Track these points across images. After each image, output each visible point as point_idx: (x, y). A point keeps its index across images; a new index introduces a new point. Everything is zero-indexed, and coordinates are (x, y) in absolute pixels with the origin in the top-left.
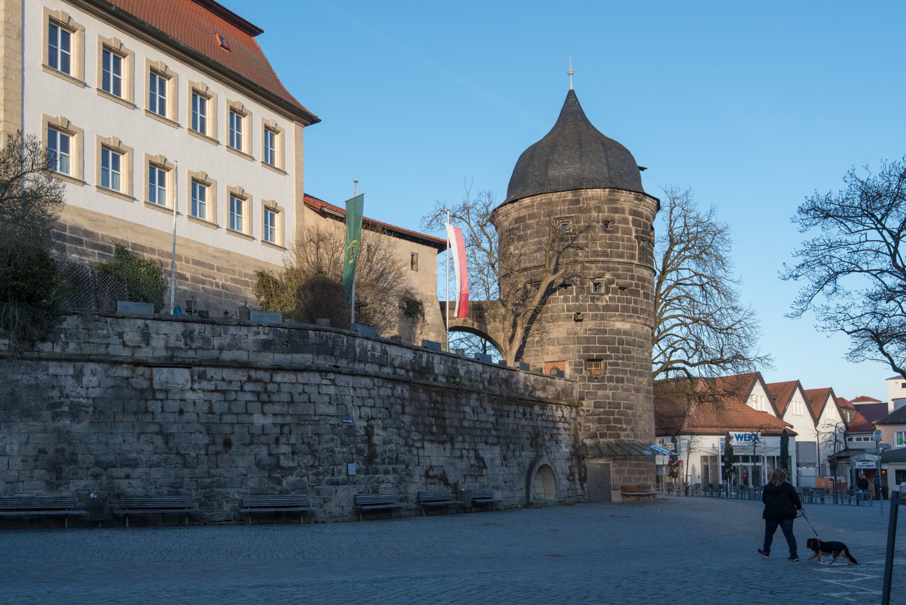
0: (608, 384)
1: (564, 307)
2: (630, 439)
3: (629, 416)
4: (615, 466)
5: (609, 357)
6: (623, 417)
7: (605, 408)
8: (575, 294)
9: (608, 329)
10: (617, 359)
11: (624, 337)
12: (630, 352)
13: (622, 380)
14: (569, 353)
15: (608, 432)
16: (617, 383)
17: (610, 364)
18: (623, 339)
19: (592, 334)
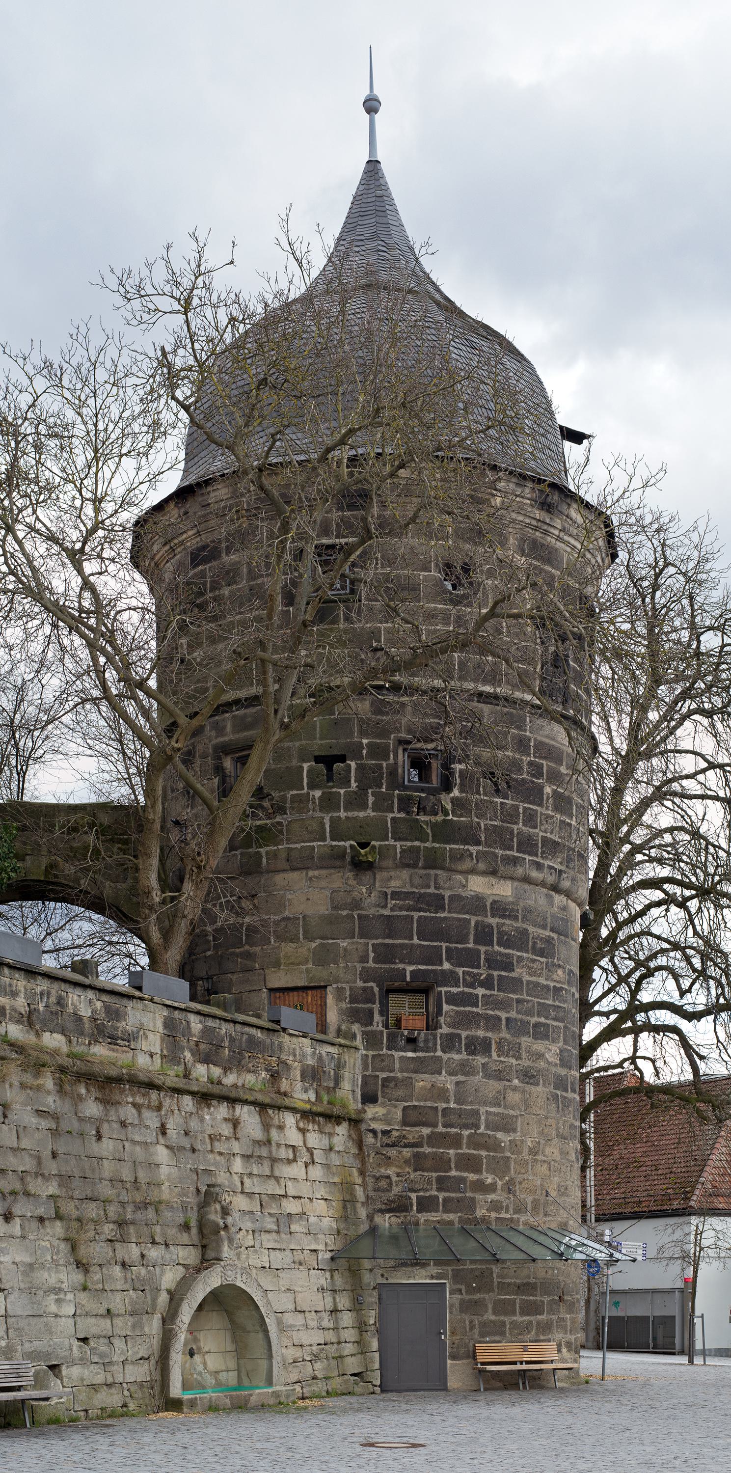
0: (445, 1057)
1: (322, 824)
2: (504, 1215)
3: (502, 1150)
4: (460, 1291)
5: (450, 978)
6: (484, 1153)
7: (435, 1126)
8: (354, 785)
9: (447, 894)
10: (472, 986)
11: (494, 921)
12: (509, 967)
13: (485, 1046)
14: (336, 962)
15: (442, 1196)
16: (472, 1053)
17: (453, 999)
18: (490, 926)
19: (401, 908)
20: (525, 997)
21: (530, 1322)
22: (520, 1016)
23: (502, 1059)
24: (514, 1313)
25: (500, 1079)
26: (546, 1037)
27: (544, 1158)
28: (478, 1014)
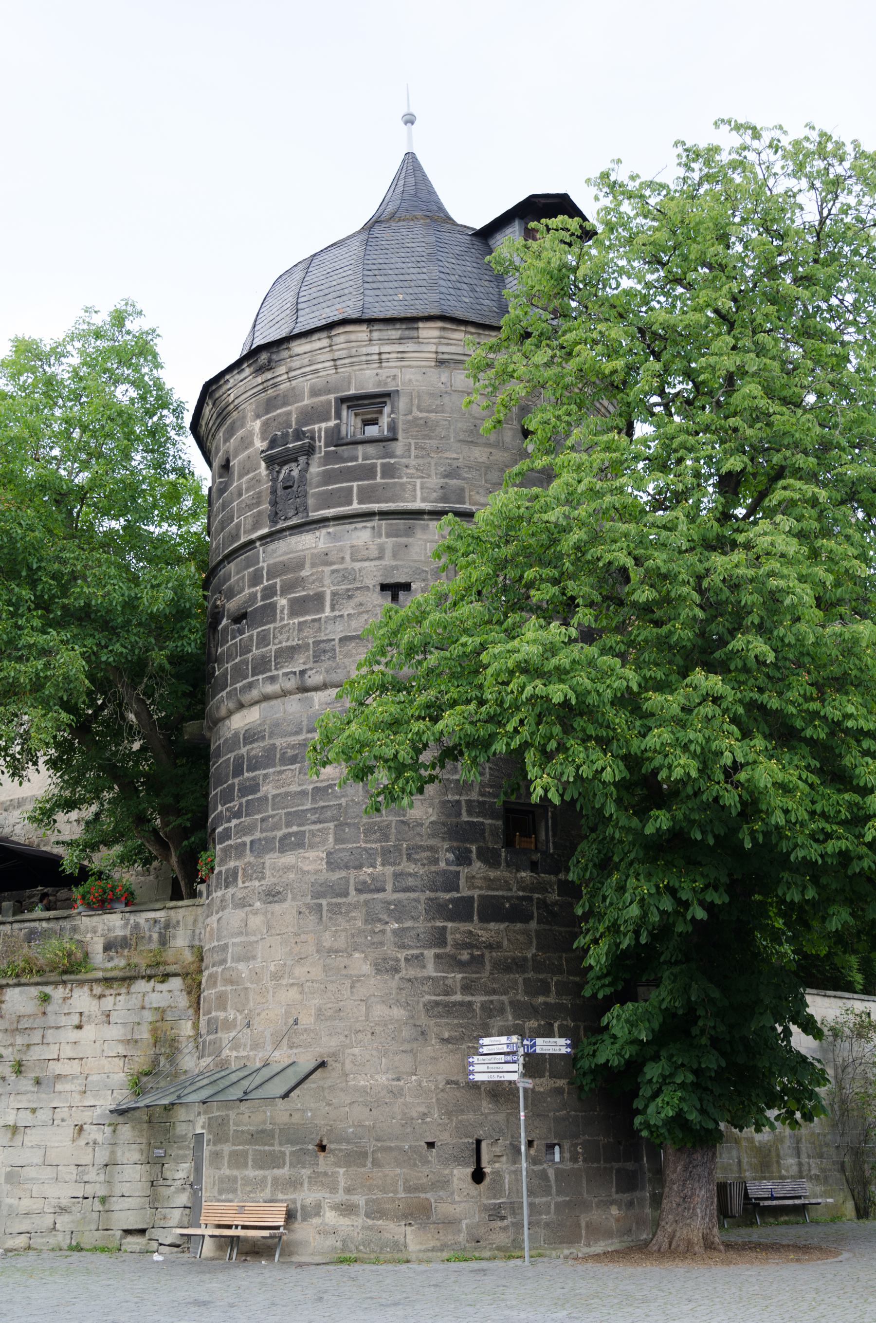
6: (229, 988)
20: (271, 812)
21: (265, 1177)
22: (264, 835)
24: (245, 1165)
25: (245, 906)
26: (300, 845)
27: (291, 981)
28: (231, 846)
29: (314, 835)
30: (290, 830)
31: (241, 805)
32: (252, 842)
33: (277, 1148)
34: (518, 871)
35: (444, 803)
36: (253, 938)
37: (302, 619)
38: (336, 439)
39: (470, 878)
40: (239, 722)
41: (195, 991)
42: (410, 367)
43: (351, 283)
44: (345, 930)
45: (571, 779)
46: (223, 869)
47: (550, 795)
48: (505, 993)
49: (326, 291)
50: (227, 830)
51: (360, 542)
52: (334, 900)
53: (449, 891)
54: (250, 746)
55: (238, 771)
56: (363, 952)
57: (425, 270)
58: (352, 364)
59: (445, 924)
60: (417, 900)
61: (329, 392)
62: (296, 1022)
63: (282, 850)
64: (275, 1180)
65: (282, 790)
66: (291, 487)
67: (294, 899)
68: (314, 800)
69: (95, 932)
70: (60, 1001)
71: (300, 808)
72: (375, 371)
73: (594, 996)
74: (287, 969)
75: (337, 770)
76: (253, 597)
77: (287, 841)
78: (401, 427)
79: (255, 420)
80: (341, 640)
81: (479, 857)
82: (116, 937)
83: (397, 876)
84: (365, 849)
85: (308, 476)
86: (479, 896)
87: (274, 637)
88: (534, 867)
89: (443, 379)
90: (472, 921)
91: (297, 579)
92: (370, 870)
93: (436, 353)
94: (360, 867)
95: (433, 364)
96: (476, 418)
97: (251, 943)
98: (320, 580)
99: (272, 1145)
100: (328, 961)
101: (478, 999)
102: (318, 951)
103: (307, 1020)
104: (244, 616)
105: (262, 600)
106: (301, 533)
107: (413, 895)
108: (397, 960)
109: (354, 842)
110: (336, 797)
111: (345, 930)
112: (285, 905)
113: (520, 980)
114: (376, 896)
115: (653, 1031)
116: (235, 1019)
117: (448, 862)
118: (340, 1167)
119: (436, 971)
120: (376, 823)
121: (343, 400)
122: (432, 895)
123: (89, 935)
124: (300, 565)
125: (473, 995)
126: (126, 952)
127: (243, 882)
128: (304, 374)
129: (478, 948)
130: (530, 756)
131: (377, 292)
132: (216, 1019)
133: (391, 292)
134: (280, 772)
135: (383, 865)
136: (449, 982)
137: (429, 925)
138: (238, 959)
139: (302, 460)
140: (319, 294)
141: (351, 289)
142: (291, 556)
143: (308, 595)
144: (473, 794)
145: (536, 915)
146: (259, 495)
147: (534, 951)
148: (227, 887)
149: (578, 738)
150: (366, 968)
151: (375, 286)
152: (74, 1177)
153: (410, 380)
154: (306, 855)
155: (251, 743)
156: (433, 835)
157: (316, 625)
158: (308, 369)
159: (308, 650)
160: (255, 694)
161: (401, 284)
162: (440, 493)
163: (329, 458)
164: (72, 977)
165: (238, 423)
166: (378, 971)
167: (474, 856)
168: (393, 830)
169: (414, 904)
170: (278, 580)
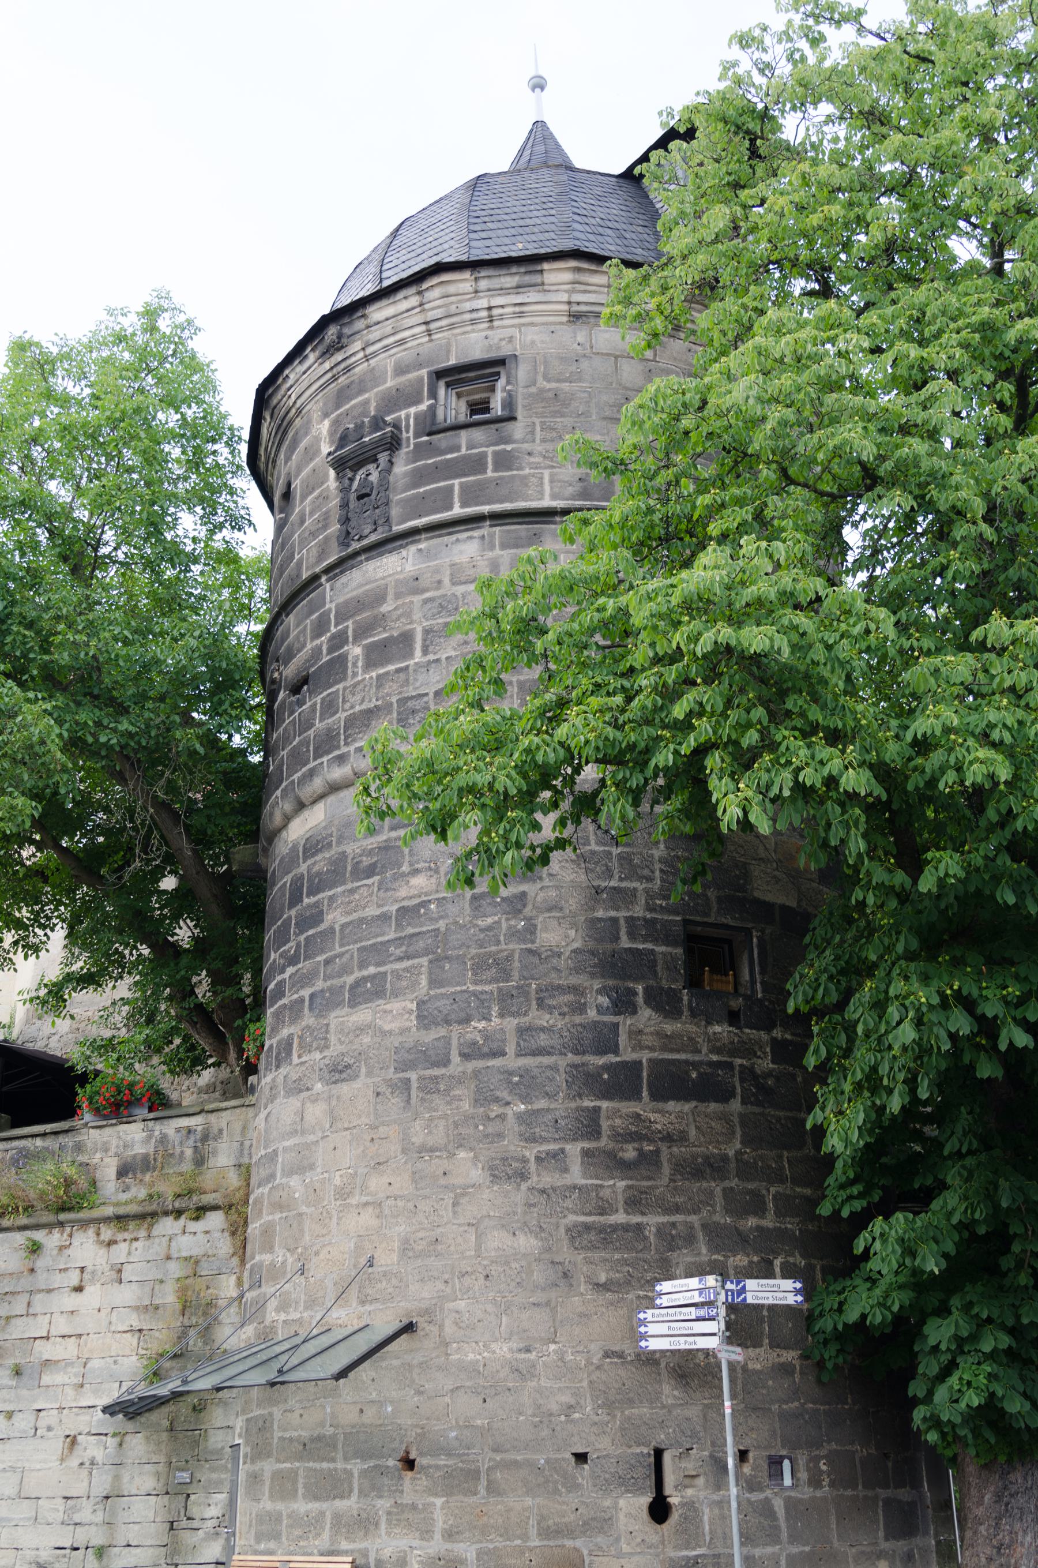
6: (277, 1216)
20: (338, 950)
21: (322, 1513)
22: (329, 983)
23: (303, 1059)
24: (293, 1495)
25: (301, 1091)
26: (379, 993)
27: (364, 1199)
29: (399, 977)
30: (365, 973)
31: (298, 945)
32: (312, 996)
33: (340, 1465)
34: (709, 1023)
35: (593, 922)
36: (312, 1138)
37: (381, 671)
38: (431, 427)
39: (635, 1034)
40: (298, 830)
41: (238, 1230)
42: (532, 324)
43: (453, 235)
44: (444, 1117)
45: (786, 793)
46: (274, 1041)
47: (752, 818)
48: (696, 1211)
49: (419, 251)
50: (281, 984)
51: (464, 559)
52: (428, 1072)
53: (603, 1053)
54: (313, 860)
55: (296, 898)
56: (471, 1149)
57: (553, 212)
58: (452, 327)
59: (598, 1103)
60: (554, 1068)
61: (420, 366)
62: (371, 1263)
63: (353, 1004)
64: (337, 1517)
65: (355, 916)
66: (368, 495)
67: (369, 1074)
68: (399, 926)
69: (106, 1150)
70: (55, 1252)
71: (379, 939)
72: (484, 334)
73: (836, 1213)
74: (358, 1181)
75: (433, 880)
76: (317, 652)
77: (360, 990)
78: (520, 402)
79: (322, 421)
80: (437, 694)
81: (647, 1002)
82: (135, 1156)
83: (522, 1031)
84: (474, 994)
85: (391, 478)
86: (650, 1060)
87: (344, 701)
88: (733, 1018)
89: (580, 338)
90: (639, 1098)
91: (375, 617)
92: (481, 1025)
93: (569, 303)
94: (467, 1020)
95: (565, 319)
96: (627, 389)
97: (307, 1146)
98: (408, 614)
99: (333, 1460)
100: (419, 1165)
101: (653, 1221)
102: (404, 1151)
103: (387, 1258)
104: (305, 681)
105: (328, 654)
106: (382, 554)
107: (546, 1060)
108: (525, 1161)
109: (458, 984)
110: (431, 919)
111: (444, 1117)
112: (357, 1084)
113: (718, 1191)
114: (491, 1063)
115: (946, 1256)
116: (284, 1262)
117: (600, 1010)
118: (436, 1495)
119: (585, 1176)
120: (490, 955)
121: (439, 374)
122: (577, 1059)
123: (98, 1155)
124: (380, 597)
125: (643, 1214)
126: (147, 1177)
127: (300, 1057)
128: (386, 348)
129: (650, 1140)
130: (714, 761)
131: (488, 243)
132: (260, 1264)
133: (507, 241)
134: (352, 891)
135: (501, 1015)
136: (606, 1193)
137: (573, 1105)
138: (289, 1173)
139: (383, 457)
140: (409, 256)
141: (452, 243)
142: (367, 587)
143: (392, 636)
144: (637, 908)
145: (739, 1090)
146: (326, 516)
147: (738, 1146)
148: (278, 1067)
149: (794, 728)
150: (477, 1174)
151: (484, 235)
152: (60, 1516)
153: (533, 342)
154: (388, 1007)
155: (314, 855)
156: (577, 970)
157: (402, 676)
158: (391, 340)
159: (390, 712)
160: (318, 784)
161: (521, 231)
162: (578, 487)
163: (420, 452)
164: (71, 1216)
165: (302, 432)
166: (495, 1178)
167: (640, 999)
168: (516, 964)
169: (549, 1073)
170: (350, 623)
